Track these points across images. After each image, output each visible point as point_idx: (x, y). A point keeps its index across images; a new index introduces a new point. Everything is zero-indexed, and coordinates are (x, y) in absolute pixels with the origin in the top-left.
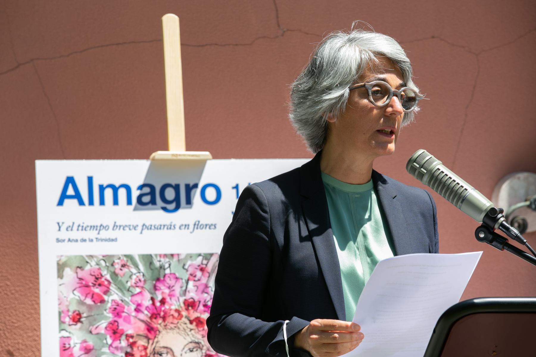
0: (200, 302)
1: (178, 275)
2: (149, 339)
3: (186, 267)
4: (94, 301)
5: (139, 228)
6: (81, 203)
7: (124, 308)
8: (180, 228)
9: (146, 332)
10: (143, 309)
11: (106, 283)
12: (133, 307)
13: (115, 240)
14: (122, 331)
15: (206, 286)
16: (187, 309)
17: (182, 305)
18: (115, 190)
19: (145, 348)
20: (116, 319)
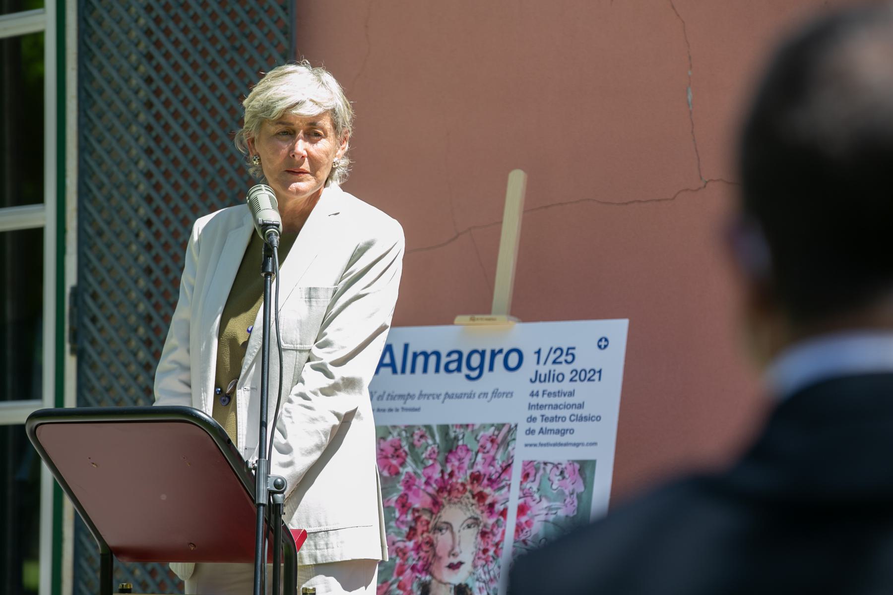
0: (485, 475)
1: (469, 446)
2: (432, 513)
3: (478, 438)
4: (390, 473)
5: (442, 397)
6: (395, 371)
7: (415, 480)
8: (479, 397)
9: (431, 506)
10: (432, 482)
11: (403, 454)
12: (423, 480)
13: (417, 410)
14: (410, 504)
15: (494, 459)
16: (472, 483)
17: (468, 478)
18: (426, 355)
19: (428, 523)
20: (407, 492)
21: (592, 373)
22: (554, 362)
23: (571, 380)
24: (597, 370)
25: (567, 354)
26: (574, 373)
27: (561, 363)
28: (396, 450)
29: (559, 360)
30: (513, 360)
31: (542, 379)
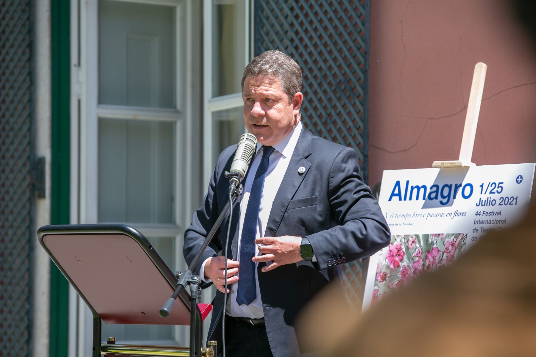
5: (425, 216)
6: (400, 199)
11: (402, 254)
18: (418, 188)
21: (512, 199)
22: (491, 192)
23: (500, 204)
24: (515, 197)
25: (498, 187)
26: (502, 199)
27: (494, 193)
28: (398, 251)
29: (493, 191)
30: (467, 192)
31: (483, 204)
